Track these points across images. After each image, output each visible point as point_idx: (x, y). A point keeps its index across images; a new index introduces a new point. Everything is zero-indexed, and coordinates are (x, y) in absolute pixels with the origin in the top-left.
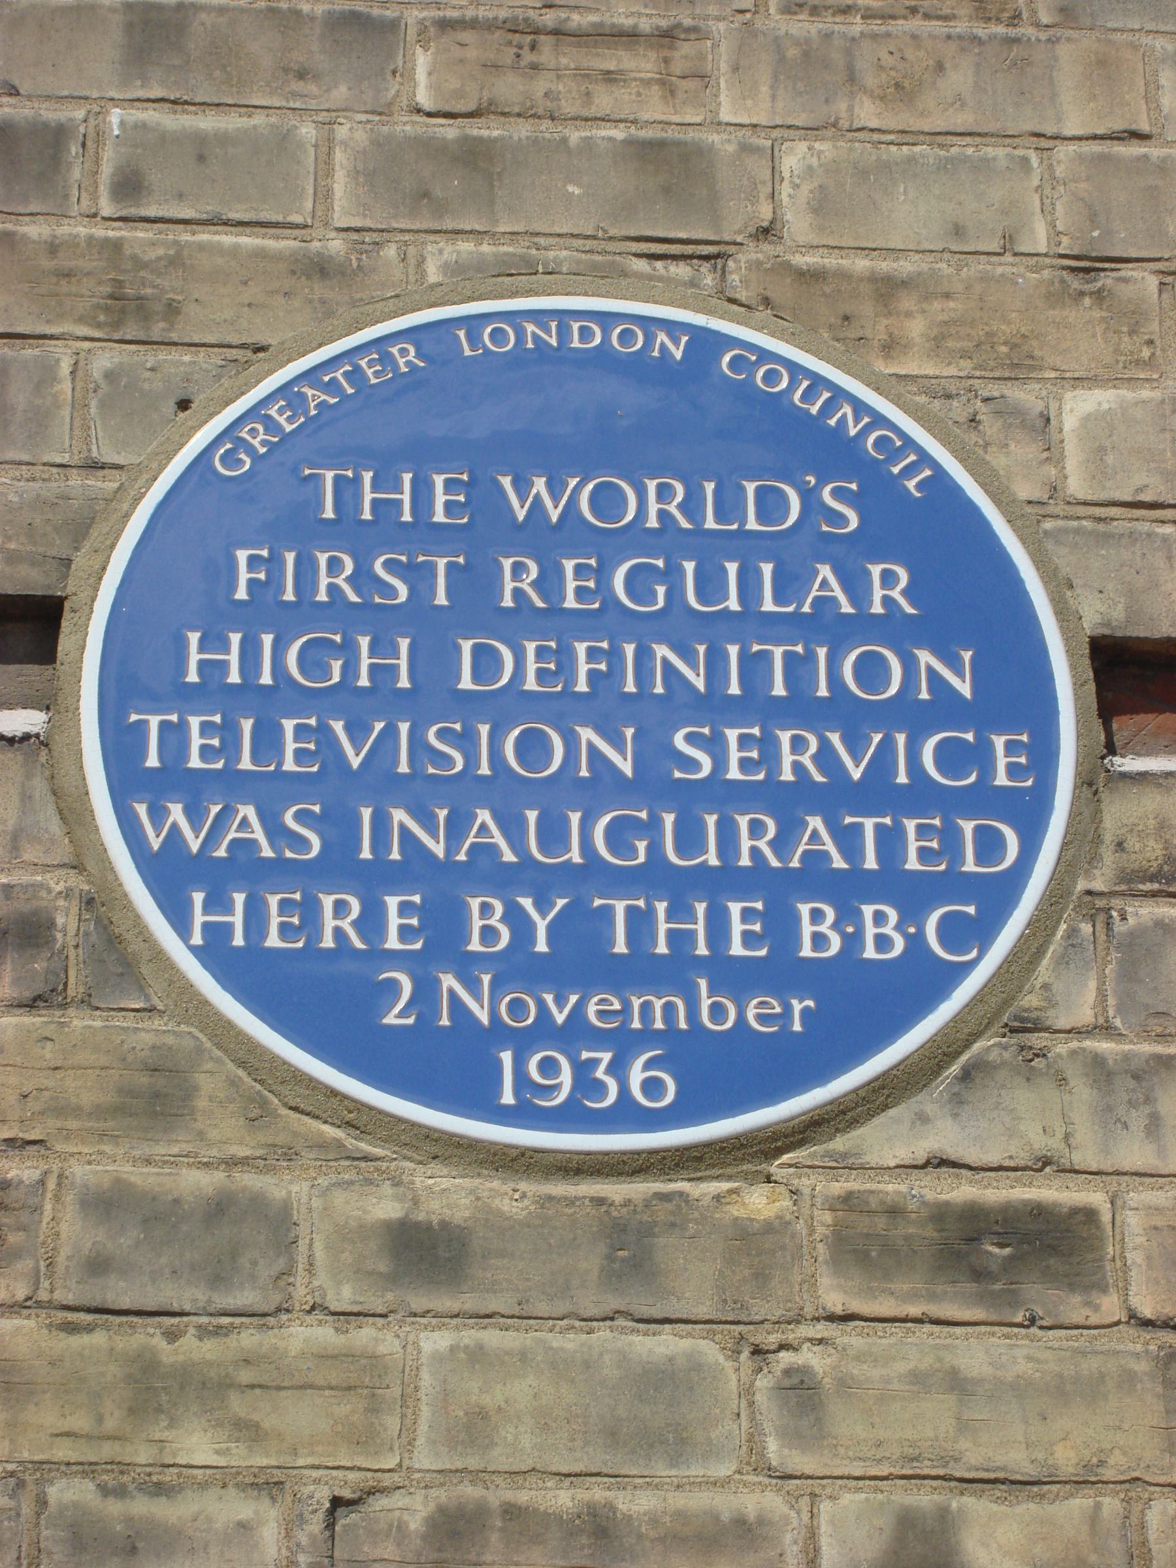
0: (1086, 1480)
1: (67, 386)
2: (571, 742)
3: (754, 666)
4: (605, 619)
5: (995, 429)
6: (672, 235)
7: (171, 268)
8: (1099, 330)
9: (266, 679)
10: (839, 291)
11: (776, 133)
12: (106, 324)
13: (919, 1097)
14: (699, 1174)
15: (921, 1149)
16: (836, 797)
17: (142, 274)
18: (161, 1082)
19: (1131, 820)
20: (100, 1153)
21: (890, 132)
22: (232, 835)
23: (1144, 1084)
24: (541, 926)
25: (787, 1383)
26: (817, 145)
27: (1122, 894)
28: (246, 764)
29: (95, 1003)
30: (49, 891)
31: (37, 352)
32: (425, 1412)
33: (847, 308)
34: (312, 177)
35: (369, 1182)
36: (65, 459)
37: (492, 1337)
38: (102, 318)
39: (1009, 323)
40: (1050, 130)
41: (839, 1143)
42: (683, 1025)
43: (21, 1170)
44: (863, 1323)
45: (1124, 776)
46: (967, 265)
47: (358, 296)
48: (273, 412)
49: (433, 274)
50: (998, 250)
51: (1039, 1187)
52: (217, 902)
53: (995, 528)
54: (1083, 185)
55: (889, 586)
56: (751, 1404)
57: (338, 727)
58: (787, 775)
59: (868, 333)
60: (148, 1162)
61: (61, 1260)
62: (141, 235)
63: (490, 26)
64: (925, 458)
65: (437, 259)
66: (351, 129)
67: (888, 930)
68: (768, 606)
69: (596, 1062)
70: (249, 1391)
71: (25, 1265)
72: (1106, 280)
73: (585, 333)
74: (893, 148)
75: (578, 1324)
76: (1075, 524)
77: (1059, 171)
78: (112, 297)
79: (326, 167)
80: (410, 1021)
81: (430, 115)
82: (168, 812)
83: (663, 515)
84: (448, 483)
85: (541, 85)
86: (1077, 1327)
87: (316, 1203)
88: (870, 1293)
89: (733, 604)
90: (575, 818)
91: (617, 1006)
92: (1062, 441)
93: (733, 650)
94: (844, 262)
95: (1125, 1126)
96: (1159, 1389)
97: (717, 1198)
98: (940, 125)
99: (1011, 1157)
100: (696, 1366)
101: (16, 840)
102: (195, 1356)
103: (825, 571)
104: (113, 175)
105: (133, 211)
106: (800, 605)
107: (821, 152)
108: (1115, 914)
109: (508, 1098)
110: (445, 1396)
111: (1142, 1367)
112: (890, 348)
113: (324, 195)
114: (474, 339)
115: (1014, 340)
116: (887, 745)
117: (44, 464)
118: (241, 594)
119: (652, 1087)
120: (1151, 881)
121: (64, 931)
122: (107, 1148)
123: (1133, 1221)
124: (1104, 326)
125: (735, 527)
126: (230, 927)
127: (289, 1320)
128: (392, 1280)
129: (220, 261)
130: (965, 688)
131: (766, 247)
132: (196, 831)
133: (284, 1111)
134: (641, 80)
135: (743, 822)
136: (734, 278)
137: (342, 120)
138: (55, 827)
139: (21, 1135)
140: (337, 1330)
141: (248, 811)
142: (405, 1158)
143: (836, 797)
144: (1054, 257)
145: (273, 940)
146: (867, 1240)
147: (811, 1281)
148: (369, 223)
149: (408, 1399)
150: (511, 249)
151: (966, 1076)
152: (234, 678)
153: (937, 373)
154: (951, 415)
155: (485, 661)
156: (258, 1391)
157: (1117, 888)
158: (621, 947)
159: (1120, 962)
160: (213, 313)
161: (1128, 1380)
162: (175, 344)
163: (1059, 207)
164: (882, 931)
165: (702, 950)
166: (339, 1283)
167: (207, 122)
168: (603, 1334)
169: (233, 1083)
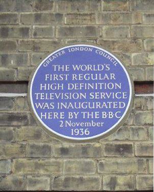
0: (130, 173)
1: (29, 57)
2: (79, 95)
3: (99, 86)
4: (84, 81)
9: (49, 89)
15: (115, 138)
16: (106, 100)
40: (131, 23)
41: (106, 138)
49: (66, 43)
52: (44, 114)
55: (113, 76)
58: (101, 98)
63: (73, 14)
64: (117, 62)
68: (100, 79)
72: (136, 40)
73: (82, 49)
79: (55, 32)
89: (96, 79)
90: (80, 103)
97: (94, 145)
100: (91, 162)
101: (24, 108)
103: (106, 75)
109: (72, 134)
110: (66, 166)
112: (114, 49)
113: (55, 35)
114: (70, 50)
119: (87, 133)
123: (135, 146)
130: (120, 88)
135: (97, 103)
138: (27, 106)
143: (106, 100)
145: (49, 118)
146: (109, 149)
149: (62, 167)
152: (45, 89)
155: (71, 86)
160: (43, 48)
164: (111, 115)
167: (43, 27)
168: (82, 159)
169: (45, 133)
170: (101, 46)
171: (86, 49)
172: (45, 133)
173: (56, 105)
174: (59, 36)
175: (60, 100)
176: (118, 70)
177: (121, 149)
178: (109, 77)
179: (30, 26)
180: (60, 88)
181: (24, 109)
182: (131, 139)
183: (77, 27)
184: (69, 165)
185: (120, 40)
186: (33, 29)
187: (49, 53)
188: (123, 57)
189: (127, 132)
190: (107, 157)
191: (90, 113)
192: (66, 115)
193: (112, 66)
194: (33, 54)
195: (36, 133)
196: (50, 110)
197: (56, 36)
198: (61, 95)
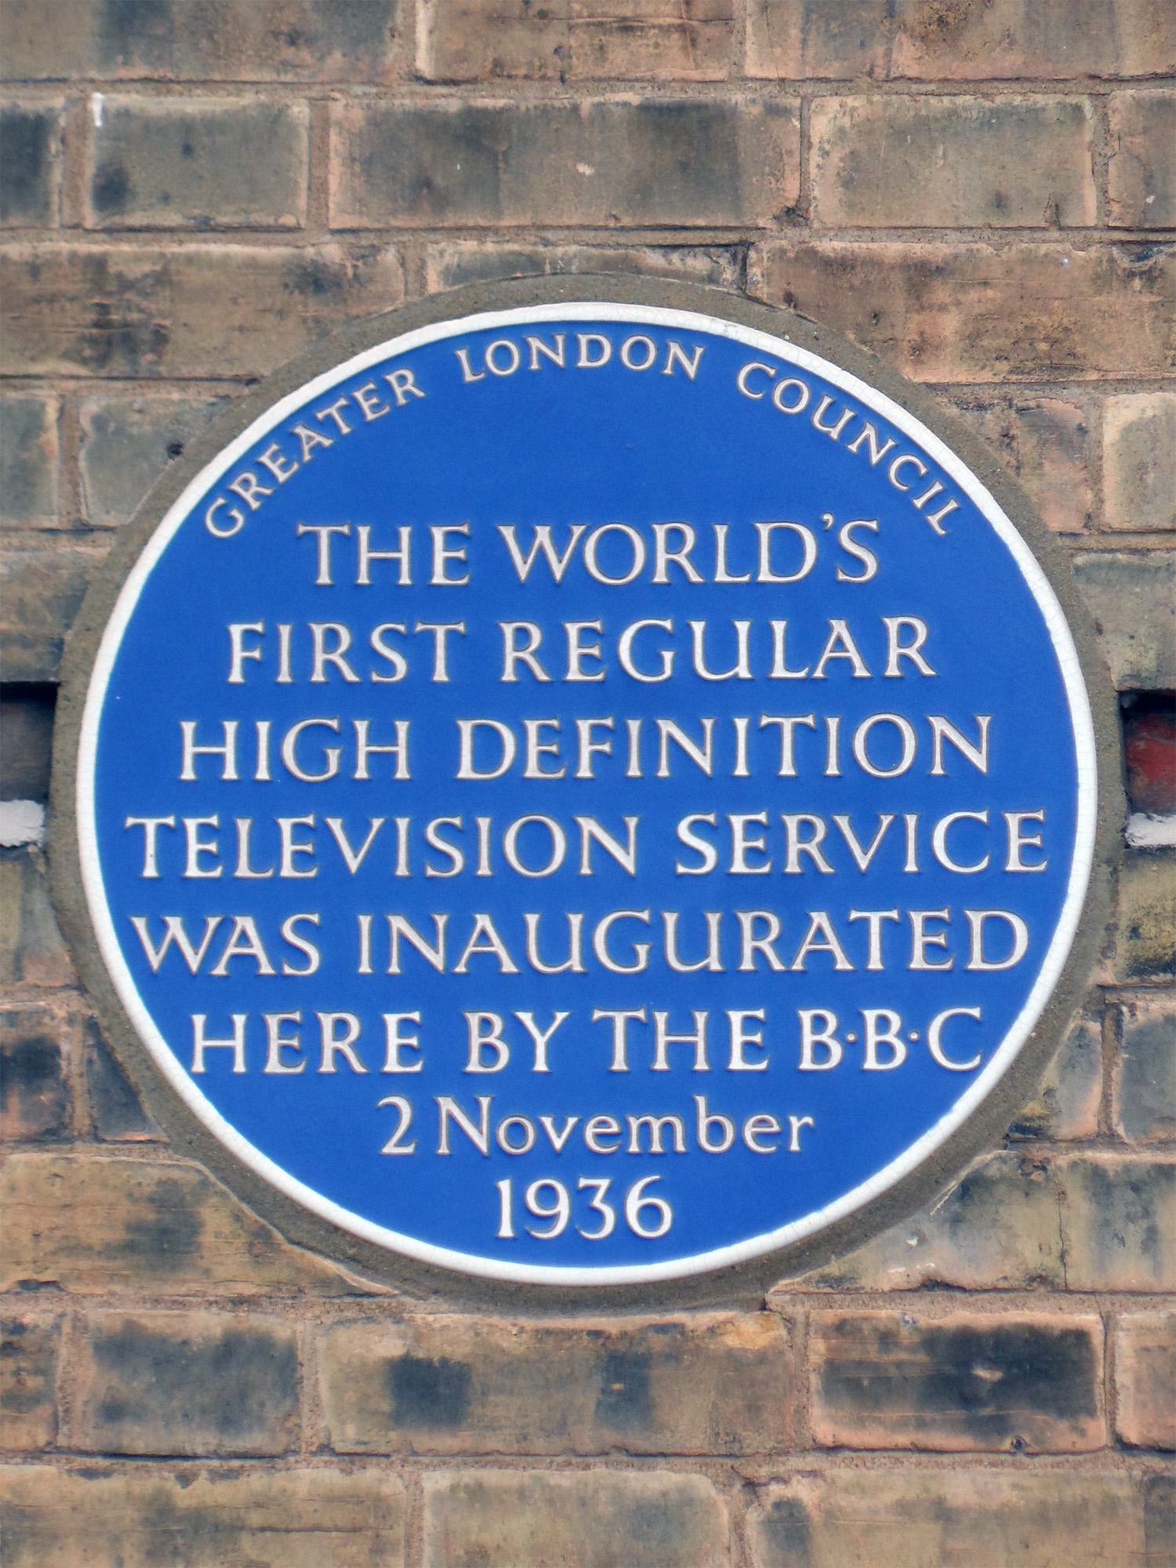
2: (573, 833)
3: (766, 741)
5: (1029, 446)
6: (689, 223)
7: (158, 288)
8: (1147, 318)
9: (263, 774)
10: (869, 282)
11: (808, 89)
12: (91, 359)
13: (916, 1216)
14: (694, 1304)
16: (844, 889)
17: (129, 296)
18: (168, 1218)
19: (1149, 901)
20: (112, 1294)
21: (931, 82)
22: (231, 950)
23: (1144, 1196)
24: (541, 1042)
25: (776, 1515)
26: (851, 101)
27: (1134, 988)
28: (243, 870)
29: (101, 1134)
30: (53, 1018)
31: (20, 395)
32: (428, 1551)
33: (876, 303)
34: (305, 168)
35: (370, 1319)
36: (53, 522)
37: (492, 1476)
38: (88, 352)
39: (1051, 314)
40: (1107, 70)
41: (834, 1268)
42: (680, 1147)
43: (34, 1314)
44: (853, 1455)
45: (1144, 852)
46: (1007, 244)
47: (354, 312)
48: (265, 459)
49: (434, 285)
50: (1043, 224)
51: (1032, 1310)
52: (220, 1026)
53: (1022, 569)
54: (1138, 140)
55: (908, 644)
56: (741, 1538)
57: (335, 825)
59: (898, 333)
60: (157, 1301)
61: (78, 1405)
62: (125, 248)
64: (953, 489)
65: (442, 256)
66: (346, 106)
67: (890, 1038)
69: (592, 1189)
70: (260, 1535)
71: (44, 1410)
72: (1160, 258)
73: (595, 348)
74: (933, 101)
75: (574, 1460)
76: (1108, 556)
77: (1115, 123)
78: (97, 325)
79: (319, 149)
80: (409, 1150)
81: (429, 83)
82: (164, 926)
83: (674, 567)
84: (449, 536)
85: (550, 40)
86: (1064, 1453)
87: (321, 1343)
88: (861, 1423)
89: (743, 671)
90: (576, 920)
91: (615, 1128)
92: (1100, 458)
93: (741, 724)
94: (873, 246)
95: (1122, 1241)
96: (1141, 1514)
97: (711, 1331)
98: (985, 70)
99: (1005, 1278)
100: (687, 1500)
102: (209, 1500)
103: (839, 628)
104: (97, 176)
105: (117, 220)
106: (813, 670)
107: (854, 109)
108: (1125, 1009)
110: (446, 1538)
111: (1124, 1492)
112: (921, 350)
113: (318, 189)
114: (477, 363)
115: (1056, 335)
116: (899, 826)
117: (32, 529)
118: (236, 676)
119: (650, 1214)
120: (1165, 971)
121: (69, 1059)
122: (117, 1288)
123: (1124, 1343)
124: (1153, 313)
125: (746, 579)
126: (230, 1051)
127: (297, 1462)
128: (397, 1419)
129: (209, 275)
130: (979, 759)
131: (790, 232)
132: (195, 944)
133: (287, 1247)
134: (660, 27)
135: (746, 920)
136: (755, 272)
137: (337, 95)
138: (56, 944)
139: (35, 1277)
140: (342, 1471)
141: (246, 923)
142: (405, 1293)
143: (844, 889)
144: (1102, 230)
145: (274, 1066)
147: (802, 1411)
148: (365, 222)
149: (411, 1540)
150: (516, 247)
151: (967, 1190)
152: (230, 773)
153: (971, 380)
154: (983, 430)
155: (488, 747)
156: (268, 1534)
157: (1129, 981)
158: (619, 1064)
159: (1128, 1064)
160: (202, 335)
161: (1111, 1506)
162: (162, 379)
163: (1112, 169)
164: (884, 1035)
165: (701, 1065)
166: (343, 1423)
167: (195, 105)
168: (600, 1472)
170: (785, 311)
171: (639, 350)
172: (238, 1217)
173: (338, 941)
174: (359, 203)
175: (379, 888)
176: (958, 579)
177: (985, 1374)
178: (874, 650)
179: (58, 102)
180: (383, 763)
181: (18, 972)
182: (1080, 1273)
183: (545, 113)
184: (474, 1528)
185: (986, 249)
186: (82, 124)
187: (261, 389)
188: (1023, 437)
189: (1047, 1205)
190: (835, 1449)
191: (682, 1023)
192: (442, 1045)
193: (899, 532)
194: (91, 407)
195: (150, 1216)
196: (282, 991)
197: (330, 208)
198: (389, 832)
